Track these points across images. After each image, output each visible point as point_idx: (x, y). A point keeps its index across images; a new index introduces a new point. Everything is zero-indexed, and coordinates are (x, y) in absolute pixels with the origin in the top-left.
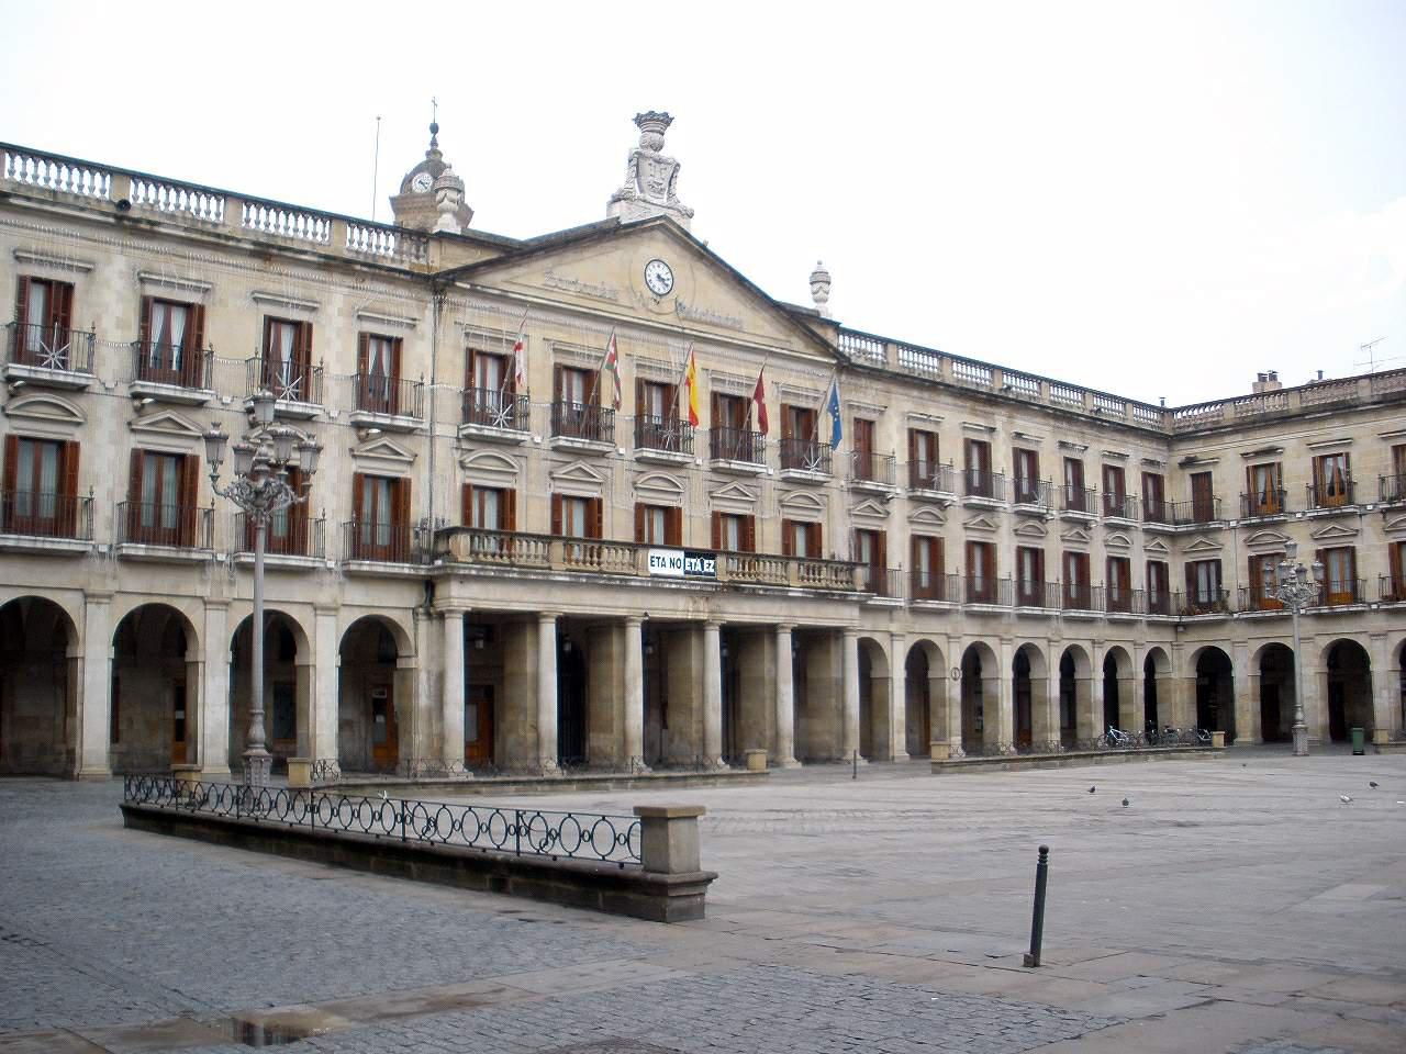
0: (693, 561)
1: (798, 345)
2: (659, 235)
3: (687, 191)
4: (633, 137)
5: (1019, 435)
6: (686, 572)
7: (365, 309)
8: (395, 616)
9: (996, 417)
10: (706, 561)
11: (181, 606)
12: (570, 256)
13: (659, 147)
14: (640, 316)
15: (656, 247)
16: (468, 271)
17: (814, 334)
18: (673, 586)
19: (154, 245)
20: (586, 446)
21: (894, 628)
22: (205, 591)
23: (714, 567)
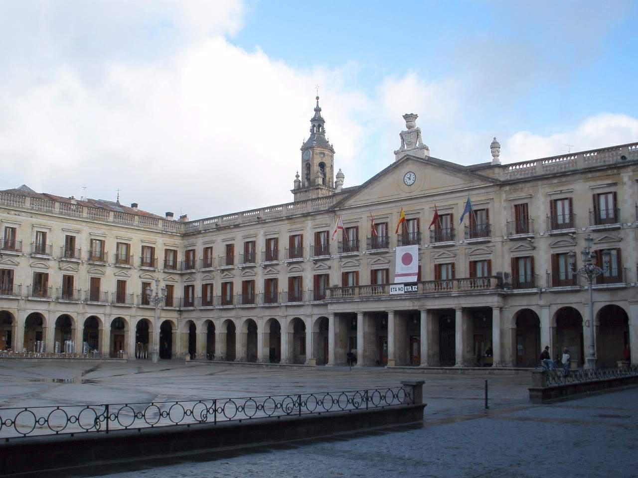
0: (408, 287)
1: (478, 183)
2: (410, 162)
3: (425, 139)
6: (405, 292)
7: (317, 225)
9: (622, 175)
10: (413, 287)
12: (376, 184)
14: (404, 196)
15: (410, 167)
16: (339, 204)
17: (480, 176)
18: (398, 298)
19: (266, 225)
20: (375, 252)
21: (542, 302)
22: (281, 314)
23: (417, 288)
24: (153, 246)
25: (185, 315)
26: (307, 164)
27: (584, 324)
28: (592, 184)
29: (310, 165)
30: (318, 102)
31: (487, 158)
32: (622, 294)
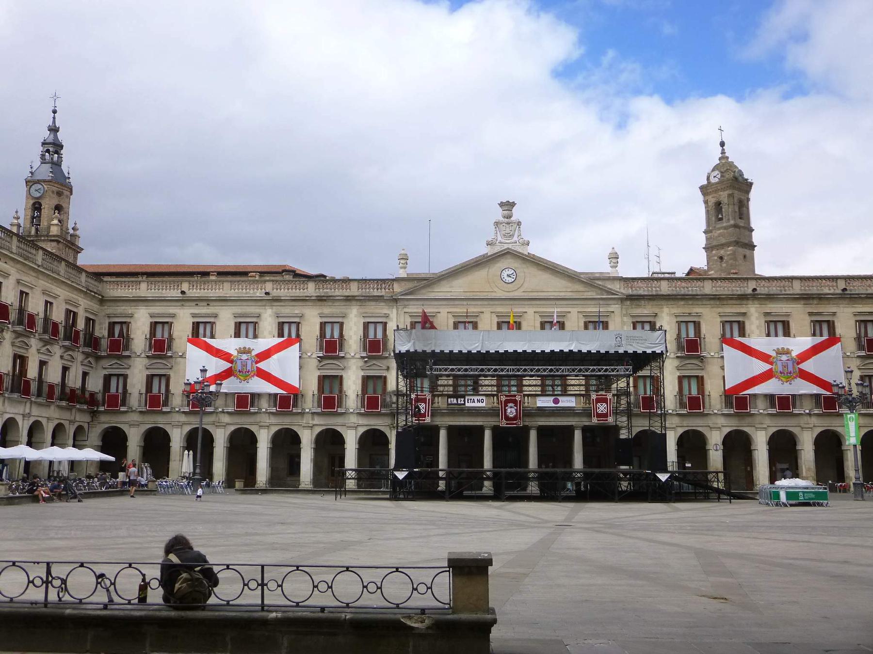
2: (508, 256)
4: (498, 214)
5: (767, 314)
8: (382, 429)
11: (295, 428)
13: (510, 217)
14: (500, 294)
24: (75, 310)
25: (103, 418)
26: (34, 204)
27: (722, 447)
28: (720, 310)
29: (40, 205)
30: (54, 118)
31: (603, 267)
32: (748, 420)
